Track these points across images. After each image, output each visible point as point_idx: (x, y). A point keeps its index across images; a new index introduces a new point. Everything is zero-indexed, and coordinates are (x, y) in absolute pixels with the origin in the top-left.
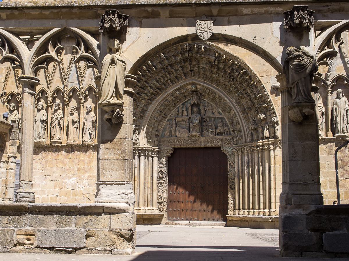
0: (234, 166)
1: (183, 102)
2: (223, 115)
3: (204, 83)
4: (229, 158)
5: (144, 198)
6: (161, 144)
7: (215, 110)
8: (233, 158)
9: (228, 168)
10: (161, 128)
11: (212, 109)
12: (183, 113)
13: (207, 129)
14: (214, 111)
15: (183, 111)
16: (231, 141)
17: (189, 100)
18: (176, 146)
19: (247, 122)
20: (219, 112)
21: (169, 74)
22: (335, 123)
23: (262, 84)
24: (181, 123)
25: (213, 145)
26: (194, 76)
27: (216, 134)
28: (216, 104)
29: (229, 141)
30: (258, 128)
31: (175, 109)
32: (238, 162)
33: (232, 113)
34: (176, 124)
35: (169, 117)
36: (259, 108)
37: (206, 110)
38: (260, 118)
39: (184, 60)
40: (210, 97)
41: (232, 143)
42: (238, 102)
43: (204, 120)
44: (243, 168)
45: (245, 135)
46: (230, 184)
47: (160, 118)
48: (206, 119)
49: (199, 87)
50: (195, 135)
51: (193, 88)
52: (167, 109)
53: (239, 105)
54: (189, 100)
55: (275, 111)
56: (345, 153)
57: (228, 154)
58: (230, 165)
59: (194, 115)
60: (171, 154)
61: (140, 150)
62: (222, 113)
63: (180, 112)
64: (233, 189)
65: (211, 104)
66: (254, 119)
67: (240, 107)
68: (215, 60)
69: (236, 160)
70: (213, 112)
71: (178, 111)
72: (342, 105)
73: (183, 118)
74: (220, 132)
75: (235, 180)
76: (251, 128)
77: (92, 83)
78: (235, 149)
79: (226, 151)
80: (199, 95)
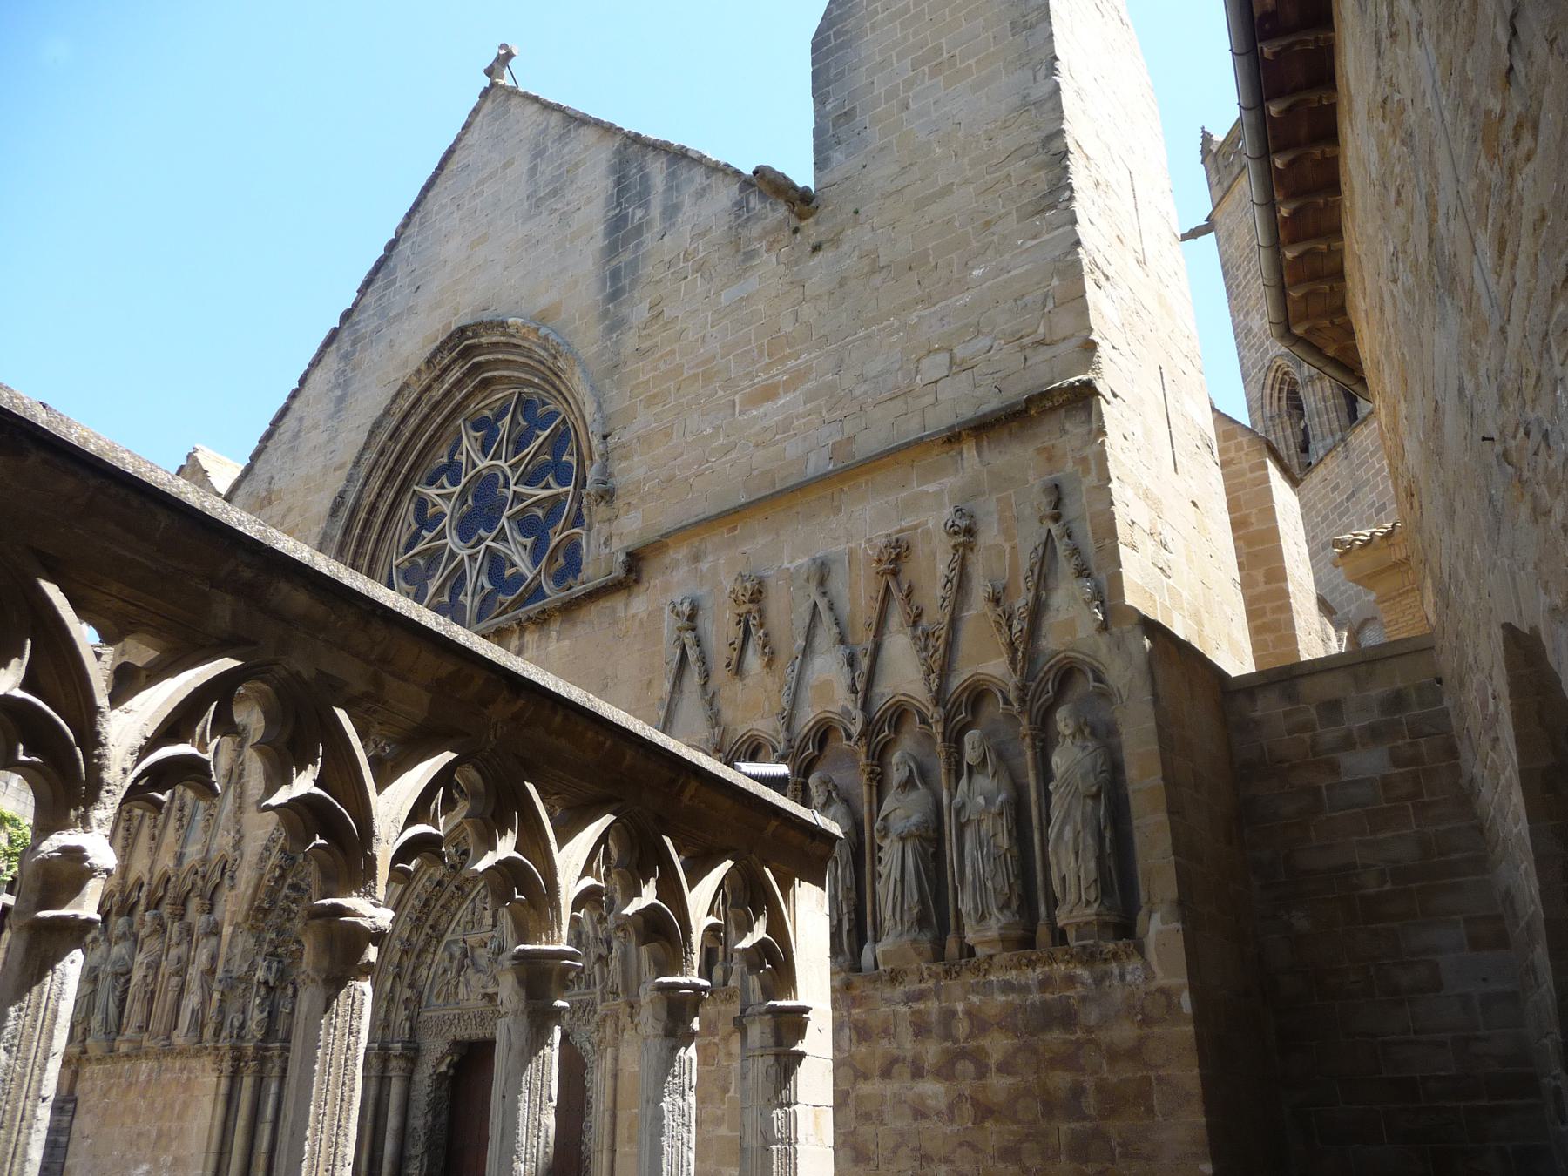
47: (419, 940)
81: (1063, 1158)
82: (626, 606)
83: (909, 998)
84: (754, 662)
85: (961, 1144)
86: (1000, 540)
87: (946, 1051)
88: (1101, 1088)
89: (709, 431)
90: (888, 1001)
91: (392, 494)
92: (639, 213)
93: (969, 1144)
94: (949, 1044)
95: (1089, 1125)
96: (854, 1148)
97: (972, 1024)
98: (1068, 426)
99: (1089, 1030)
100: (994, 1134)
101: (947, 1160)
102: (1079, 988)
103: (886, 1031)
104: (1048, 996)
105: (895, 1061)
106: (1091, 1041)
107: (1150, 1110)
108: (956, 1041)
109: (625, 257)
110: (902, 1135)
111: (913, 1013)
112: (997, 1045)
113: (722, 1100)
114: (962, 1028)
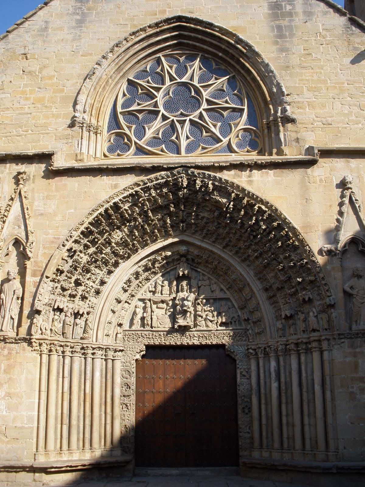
0: (248, 377)
2: (228, 295)
3: (203, 241)
4: (240, 364)
5: (100, 431)
7: (215, 286)
8: (246, 364)
9: (238, 380)
11: (210, 285)
14: (214, 287)
16: (243, 337)
17: (172, 270)
18: (152, 342)
19: (273, 306)
20: (222, 290)
23: (308, 245)
26: (185, 230)
27: (218, 326)
28: (219, 276)
29: (239, 336)
30: (296, 316)
32: (256, 370)
33: (247, 290)
34: (151, 307)
37: (200, 287)
38: (304, 299)
40: (208, 266)
41: (244, 339)
42: (260, 276)
44: (268, 380)
49: (192, 249)
50: (185, 326)
53: (259, 279)
54: (172, 270)
55: (329, 288)
57: (236, 358)
58: (241, 374)
60: (143, 357)
61: (94, 349)
62: (227, 291)
64: (247, 414)
65: (209, 278)
66: (289, 301)
67: (261, 283)
69: (253, 367)
70: (212, 290)
71: (155, 287)
73: (163, 299)
76: (286, 315)
77: (18, 233)
79: (234, 352)
80: (190, 262)
89: (346, 112)
91: (118, 77)
92: (289, 7)
109: (285, 22)
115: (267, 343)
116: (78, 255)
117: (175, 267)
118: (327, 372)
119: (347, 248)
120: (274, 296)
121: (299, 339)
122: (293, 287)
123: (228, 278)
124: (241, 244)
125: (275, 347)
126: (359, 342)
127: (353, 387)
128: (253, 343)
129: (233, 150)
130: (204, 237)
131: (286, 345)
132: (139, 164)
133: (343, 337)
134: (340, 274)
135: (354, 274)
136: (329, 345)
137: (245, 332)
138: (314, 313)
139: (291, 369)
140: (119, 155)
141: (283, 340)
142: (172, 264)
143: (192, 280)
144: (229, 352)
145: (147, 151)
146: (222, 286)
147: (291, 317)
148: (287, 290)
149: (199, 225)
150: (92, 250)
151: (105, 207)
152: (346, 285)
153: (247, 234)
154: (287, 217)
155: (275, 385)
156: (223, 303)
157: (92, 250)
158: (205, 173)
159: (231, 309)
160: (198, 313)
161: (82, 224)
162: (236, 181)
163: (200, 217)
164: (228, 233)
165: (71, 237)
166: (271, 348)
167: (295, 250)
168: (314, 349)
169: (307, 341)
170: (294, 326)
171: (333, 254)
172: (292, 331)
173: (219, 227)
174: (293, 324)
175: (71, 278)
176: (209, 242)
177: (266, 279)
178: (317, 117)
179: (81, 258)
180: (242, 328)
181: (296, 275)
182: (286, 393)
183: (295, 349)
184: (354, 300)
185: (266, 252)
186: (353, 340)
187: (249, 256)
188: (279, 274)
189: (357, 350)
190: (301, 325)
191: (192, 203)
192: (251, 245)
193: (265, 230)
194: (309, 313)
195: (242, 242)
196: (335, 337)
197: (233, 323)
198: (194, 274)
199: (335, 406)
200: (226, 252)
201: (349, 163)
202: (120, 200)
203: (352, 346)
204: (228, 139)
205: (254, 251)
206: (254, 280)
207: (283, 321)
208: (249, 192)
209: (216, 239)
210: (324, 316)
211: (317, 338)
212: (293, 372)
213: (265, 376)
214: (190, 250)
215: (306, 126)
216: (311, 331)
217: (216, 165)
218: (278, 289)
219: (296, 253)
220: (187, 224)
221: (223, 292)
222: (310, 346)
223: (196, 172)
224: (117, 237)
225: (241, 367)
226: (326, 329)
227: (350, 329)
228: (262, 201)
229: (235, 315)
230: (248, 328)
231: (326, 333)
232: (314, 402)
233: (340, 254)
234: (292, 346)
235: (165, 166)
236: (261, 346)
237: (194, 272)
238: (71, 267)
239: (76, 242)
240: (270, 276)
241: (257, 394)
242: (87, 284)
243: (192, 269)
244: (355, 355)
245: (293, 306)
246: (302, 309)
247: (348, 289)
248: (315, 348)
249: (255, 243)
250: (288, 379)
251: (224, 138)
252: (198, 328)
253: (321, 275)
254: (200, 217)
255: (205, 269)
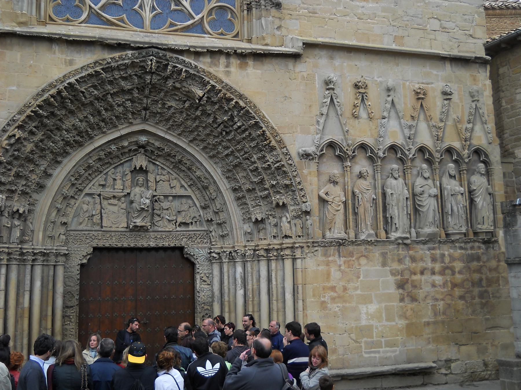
1: (116, 165)
2: (189, 192)
3: (166, 132)
6: (71, 241)
7: (175, 181)
8: (206, 268)
9: (198, 286)
10: (71, 211)
12: (114, 185)
13: (161, 216)
15: (115, 180)
19: (241, 207)
21: (106, 110)
22: (391, 217)
23: (286, 147)
24: (110, 202)
25: (172, 245)
30: (266, 219)
31: (100, 176)
32: (219, 275)
33: (212, 188)
35: (87, 190)
36: (273, 186)
37: (159, 182)
39: (137, 88)
43: (156, 198)
45: (236, 229)
46: (202, 315)
48: (158, 197)
50: (142, 227)
51: (143, 139)
52: (86, 174)
53: (227, 178)
56: (405, 264)
57: (196, 263)
59: (137, 190)
63: (110, 181)
68: (203, 96)
71: (105, 180)
72: (399, 189)
74: (184, 221)
75: (212, 306)
78: (216, 253)
79: (194, 255)
81: (477, 298)
82: (294, 66)
83: (429, 249)
84: (363, 114)
85: (447, 295)
86: (458, 101)
87: (442, 267)
88: (487, 279)
90: (422, 249)
93: (450, 295)
94: (443, 265)
95: (484, 289)
96: (411, 297)
97: (450, 259)
98: (480, 71)
99: (484, 262)
100: (457, 292)
101: (443, 300)
102: (482, 250)
103: (422, 259)
104: (473, 252)
105: (425, 269)
106: (484, 265)
107: (499, 285)
108: (445, 264)
110: (428, 292)
111: (431, 254)
112: (458, 265)
113: (357, 281)
114: (447, 260)
115: (234, 247)
116: (22, 143)
117: (130, 158)
118: (300, 280)
119: (324, 152)
120: (244, 197)
121: (270, 245)
122: (266, 189)
123: (190, 174)
124: (211, 140)
125: (243, 252)
126: (332, 251)
127: (325, 296)
128: (216, 246)
129: (206, 31)
130: (169, 129)
131: (255, 250)
132: (101, 38)
133: (317, 245)
134: (316, 179)
135: (330, 180)
136: (302, 253)
137: (207, 234)
138: (287, 218)
139: (259, 276)
140: (68, 20)
141: (251, 244)
142: (127, 156)
143: (149, 174)
144: (188, 256)
145: (105, 20)
146: (183, 182)
147: (262, 221)
148: (258, 192)
149: (164, 115)
150: (39, 136)
151: (57, 87)
152: (322, 191)
153: (219, 130)
154: (266, 116)
155: (240, 292)
156: (184, 200)
157: (39, 136)
158: (178, 58)
159: (192, 208)
160: (155, 211)
161: (30, 107)
162: (211, 70)
163: (166, 106)
164: (197, 127)
165: (14, 120)
166: (238, 253)
167: (271, 151)
168: (287, 257)
169: (279, 247)
170: (263, 231)
171: (311, 157)
172: (261, 235)
173: (187, 119)
174: (263, 228)
175: (10, 170)
176: (174, 134)
177: (235, 179)
178: (303, 3)
179: (24, 146)
180: (203, 229)
181: (270, 177)
182: (253, 301)
183: (265, 255)
184: (329, 207)
185: (239, 151)
186: (326, 248)
187: (218, 153)
188: (250, 174)
189: (330, 259)
190: (271, 230)
191: (159, 89)
192: (222, 141)
193: (239, 127)
194: (281, 218)
195: (212, 137)
196: (309, 244)
197: (194, 223)
198: (151, 167)
199: (306, 315)
200: (192, 147)
201: (332, 59)
202: (76, 80)
203: (325, 255)
204: (200, 16)
205: (224, 148)
206: (221, 179)
207: (251, 224)
208: (227, 85)
209: (183, 131)
210: (298, 222)
211: (290, 246)
212: (261, 279)
213: (229, 282)
214: (151, 141)
215: (291, 12)
216: (283, 237)
217: (192, 49)
218: (249, 191)
219: (272, 154)
220: (150, 113)
221: (183, 189)
222: (282, 253)
223: (169, 54)
224: (68, 123)
225: (201, 272)
226: (299, 236)
227: (324, 237)
228: (241, 96)
229: (197, 215)
230: (211, 230)
231: (299, 240)
232: (285, 312)
233: (317, 158)
234: (262, 253)
235: (132, 45)
236: (225, 250)
237: (151, 165)
238: (11, 156)
239: (20, 127)
240: (241, 174)
241: (220, 301)
242: (29, 177)
243: (149, 161)
244: (328, 264)
245: (263, 209)
246: (273, 213)
247: (323, 196)
248: (287, 255)
249: (228, 140)
250: (255, 287)
251: (196, 15)
252: (156, 228)
253: (298, 180)
254: (166, 106)
255: (165, 163)
